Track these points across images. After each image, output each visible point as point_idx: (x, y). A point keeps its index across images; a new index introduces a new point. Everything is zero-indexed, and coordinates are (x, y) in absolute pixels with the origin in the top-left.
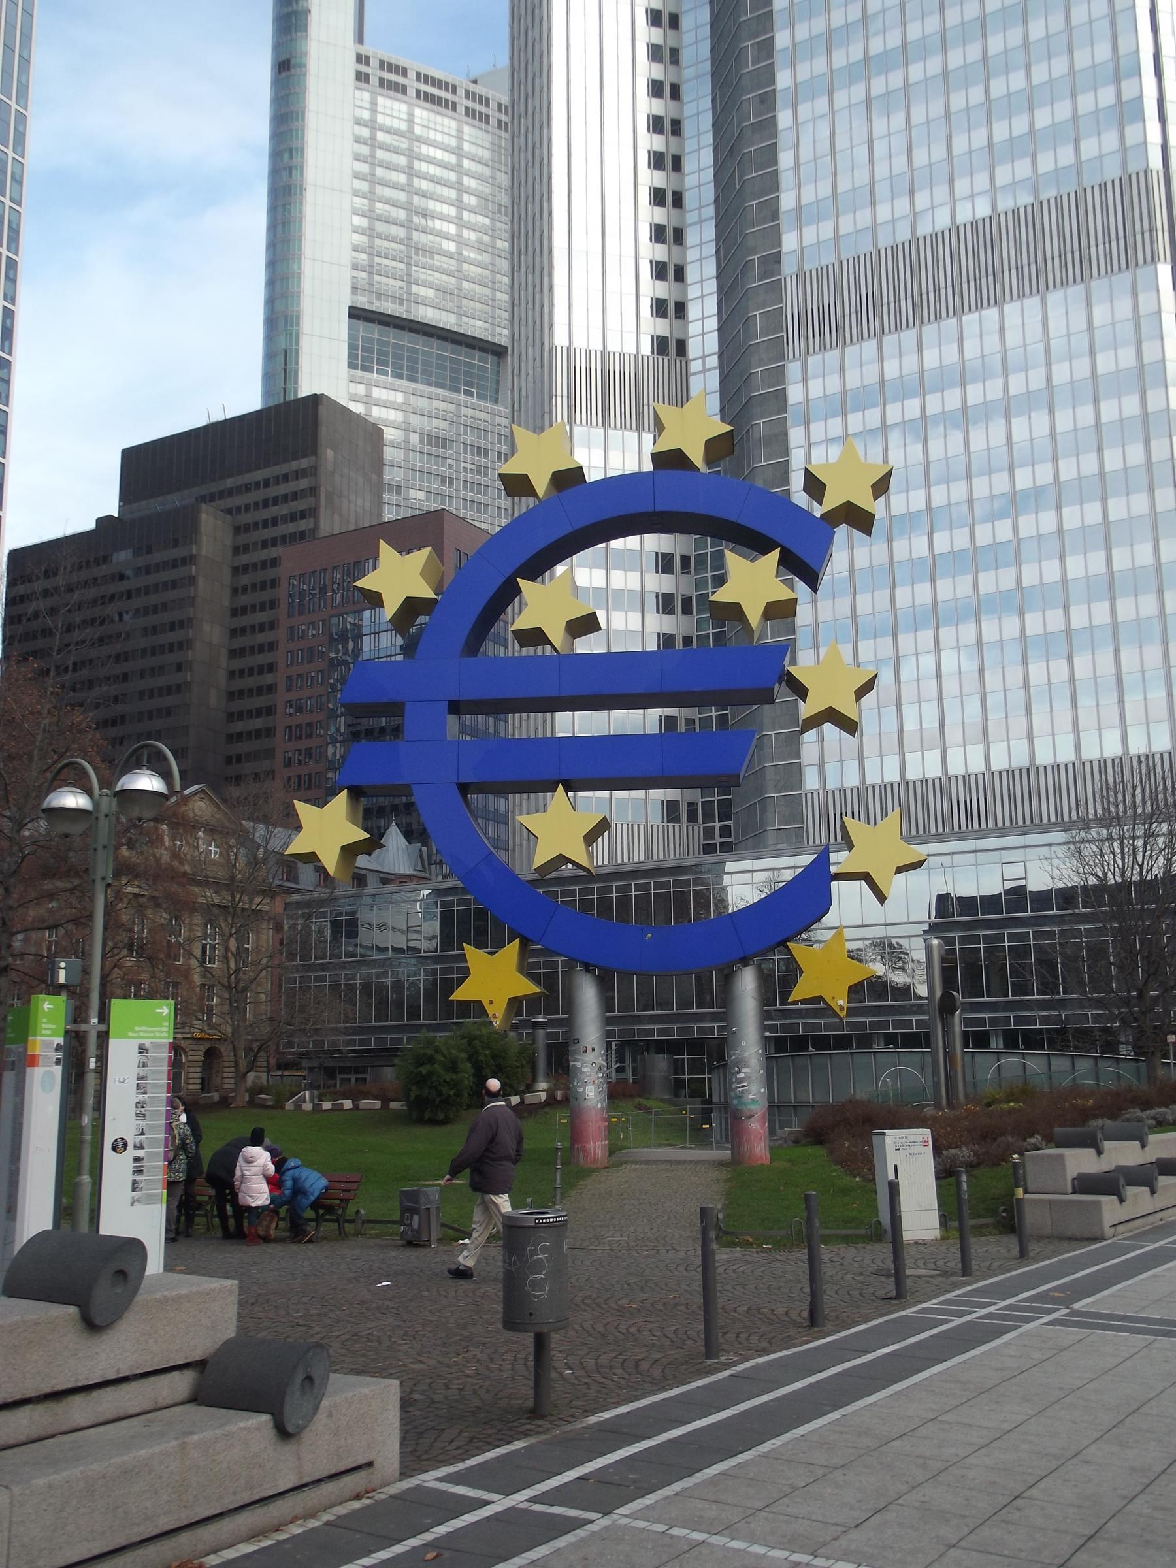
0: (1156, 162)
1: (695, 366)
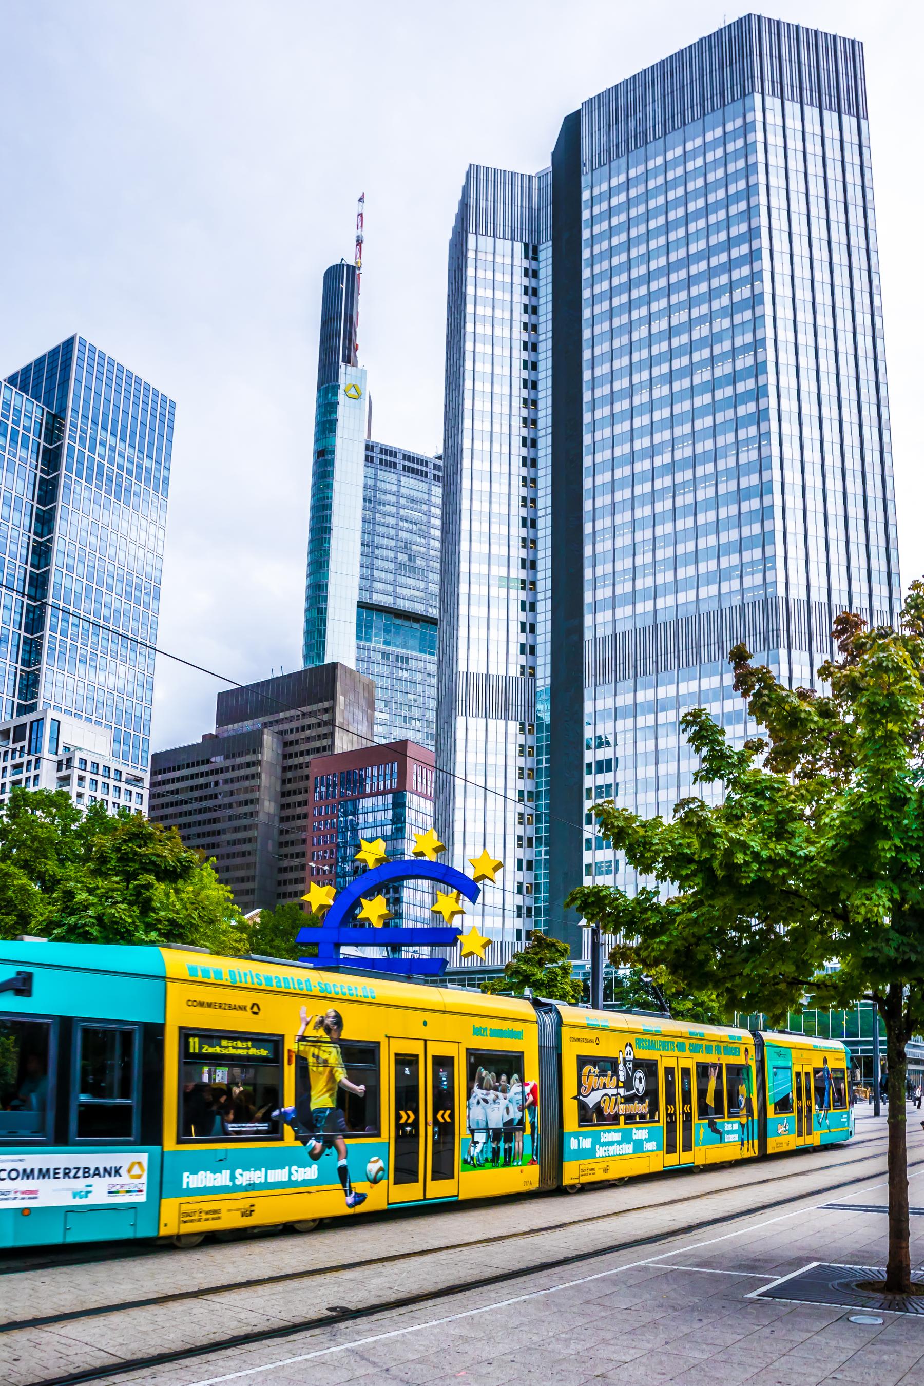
0: (781, 592)
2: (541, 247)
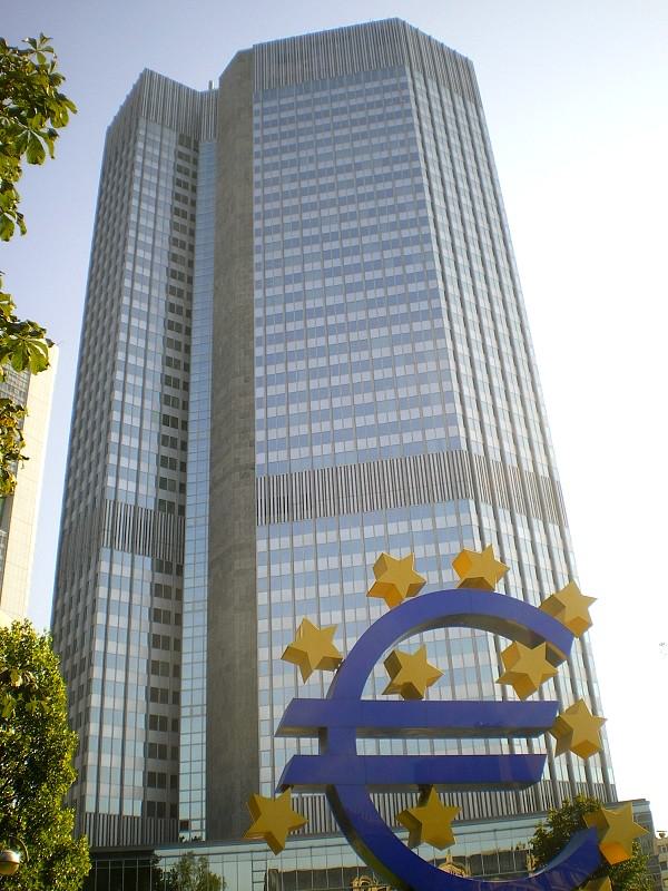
0: (464, 448)
1: (189, 522)
2: (200, 144)
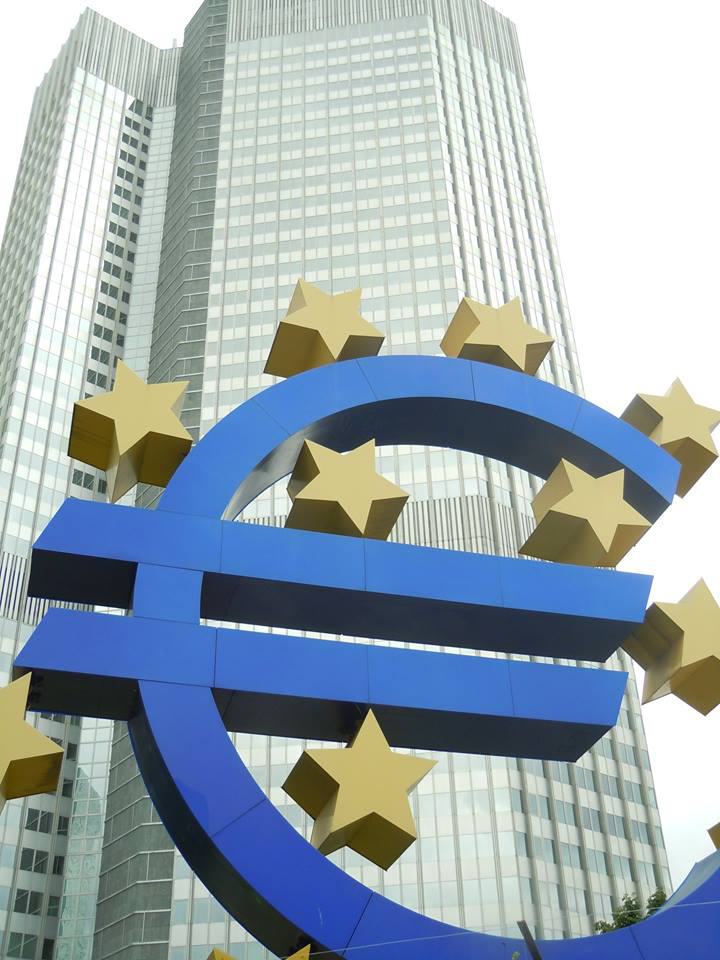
2: (156, 111)
